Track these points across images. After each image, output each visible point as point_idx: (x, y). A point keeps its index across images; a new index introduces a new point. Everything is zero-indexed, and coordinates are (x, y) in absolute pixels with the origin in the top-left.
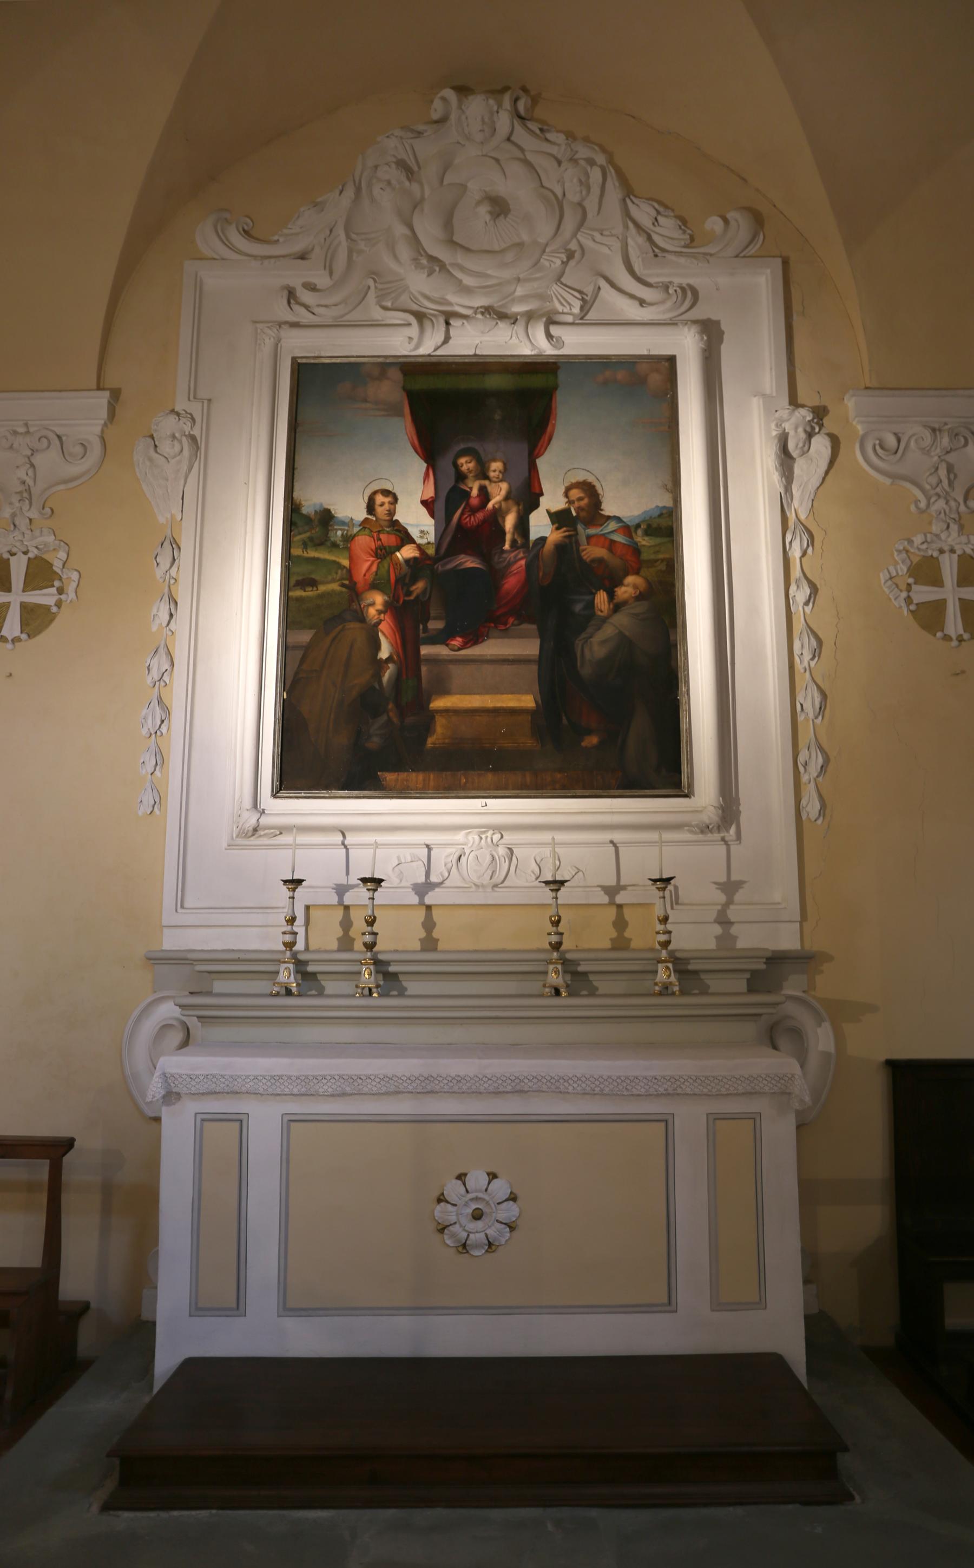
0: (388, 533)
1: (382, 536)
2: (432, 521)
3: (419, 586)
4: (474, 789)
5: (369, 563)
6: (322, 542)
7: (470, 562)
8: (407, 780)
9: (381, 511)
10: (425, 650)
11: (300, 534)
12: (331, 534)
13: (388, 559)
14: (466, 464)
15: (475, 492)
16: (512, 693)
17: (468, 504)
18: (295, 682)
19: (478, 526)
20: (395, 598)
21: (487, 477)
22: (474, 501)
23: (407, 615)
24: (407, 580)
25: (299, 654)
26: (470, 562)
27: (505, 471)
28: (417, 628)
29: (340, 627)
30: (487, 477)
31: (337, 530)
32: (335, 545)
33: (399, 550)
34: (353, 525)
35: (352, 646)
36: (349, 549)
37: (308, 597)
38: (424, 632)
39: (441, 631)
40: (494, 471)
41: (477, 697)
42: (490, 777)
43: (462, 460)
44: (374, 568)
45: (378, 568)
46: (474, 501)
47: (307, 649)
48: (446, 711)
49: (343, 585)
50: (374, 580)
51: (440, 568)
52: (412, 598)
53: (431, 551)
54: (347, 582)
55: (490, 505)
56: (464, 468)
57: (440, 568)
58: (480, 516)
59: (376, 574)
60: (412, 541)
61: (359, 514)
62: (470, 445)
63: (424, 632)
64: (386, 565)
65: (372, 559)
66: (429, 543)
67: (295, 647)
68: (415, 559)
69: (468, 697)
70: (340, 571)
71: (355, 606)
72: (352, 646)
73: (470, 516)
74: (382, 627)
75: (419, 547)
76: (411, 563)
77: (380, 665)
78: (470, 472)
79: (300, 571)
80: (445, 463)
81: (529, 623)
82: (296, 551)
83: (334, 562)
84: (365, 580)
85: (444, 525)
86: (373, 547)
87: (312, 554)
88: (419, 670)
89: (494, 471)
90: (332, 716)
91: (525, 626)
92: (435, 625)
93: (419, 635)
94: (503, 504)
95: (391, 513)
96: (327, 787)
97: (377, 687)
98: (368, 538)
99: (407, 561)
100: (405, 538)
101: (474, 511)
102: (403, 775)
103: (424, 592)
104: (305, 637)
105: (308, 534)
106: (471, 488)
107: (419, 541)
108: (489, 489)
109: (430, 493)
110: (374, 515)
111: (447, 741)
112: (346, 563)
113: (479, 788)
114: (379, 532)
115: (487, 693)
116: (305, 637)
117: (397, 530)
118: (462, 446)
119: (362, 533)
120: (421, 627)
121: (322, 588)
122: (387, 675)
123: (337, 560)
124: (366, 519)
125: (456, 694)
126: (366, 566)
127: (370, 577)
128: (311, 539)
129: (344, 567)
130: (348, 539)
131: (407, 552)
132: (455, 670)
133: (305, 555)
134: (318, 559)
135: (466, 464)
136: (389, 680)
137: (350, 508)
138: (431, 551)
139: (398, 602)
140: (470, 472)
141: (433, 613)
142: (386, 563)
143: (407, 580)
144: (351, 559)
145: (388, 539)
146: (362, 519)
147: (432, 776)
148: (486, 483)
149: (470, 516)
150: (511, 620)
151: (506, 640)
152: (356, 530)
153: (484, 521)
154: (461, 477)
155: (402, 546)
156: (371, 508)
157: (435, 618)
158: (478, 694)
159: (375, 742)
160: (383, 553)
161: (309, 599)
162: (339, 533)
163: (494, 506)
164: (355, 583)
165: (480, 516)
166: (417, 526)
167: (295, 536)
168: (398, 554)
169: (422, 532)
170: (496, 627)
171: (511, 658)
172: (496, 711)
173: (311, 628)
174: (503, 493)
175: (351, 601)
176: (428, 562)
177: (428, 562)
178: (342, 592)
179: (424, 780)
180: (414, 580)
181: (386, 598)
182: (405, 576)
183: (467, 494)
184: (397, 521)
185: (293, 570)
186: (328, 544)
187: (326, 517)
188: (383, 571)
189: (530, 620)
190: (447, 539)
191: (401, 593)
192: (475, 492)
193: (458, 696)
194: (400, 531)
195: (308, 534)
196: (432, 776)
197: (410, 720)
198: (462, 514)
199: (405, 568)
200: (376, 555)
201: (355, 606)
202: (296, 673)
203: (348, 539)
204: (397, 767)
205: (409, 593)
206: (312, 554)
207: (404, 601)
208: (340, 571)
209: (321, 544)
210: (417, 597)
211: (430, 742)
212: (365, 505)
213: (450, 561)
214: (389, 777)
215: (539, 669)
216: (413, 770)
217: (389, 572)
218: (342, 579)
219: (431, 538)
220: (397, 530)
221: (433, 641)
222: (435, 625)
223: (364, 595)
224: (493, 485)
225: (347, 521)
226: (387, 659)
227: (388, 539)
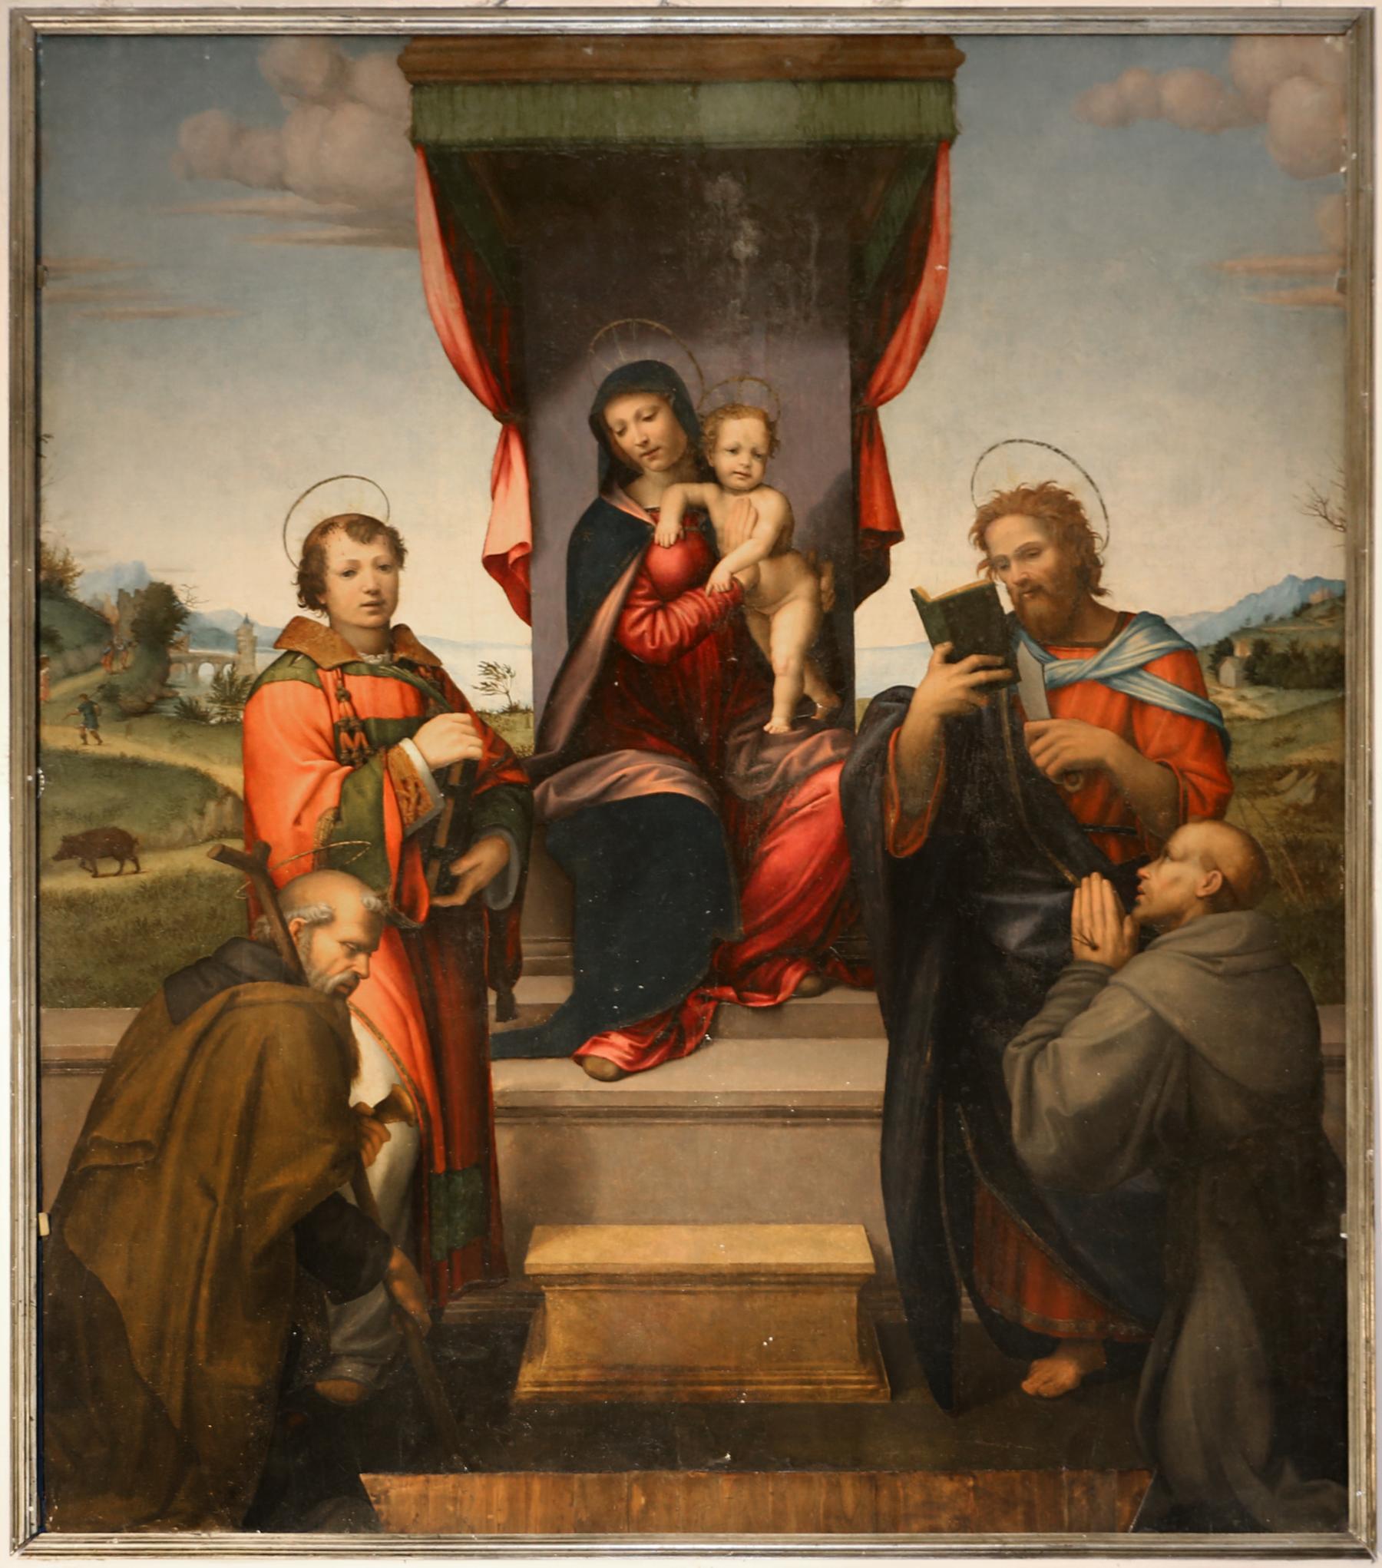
0: (373, 671)
1: (353, 683)
2: (523, 632)
3: (483, 860)
4: (672, 1528)
5: (311, 779)
6: (147, 703)
7: (651, 776)
8: (455, 1500)
9: (348, 596)
10: (509, 1078)
11: (71, 674)
12: (178, 675)
13: (375, 764)
14: (638, 423)
15: (667, 528)
16: (797, 1220)
17: (643, 570)
18: (77, 1180)
19: (680, 650)
20: (403, 902)
21: (708, 474)
22: (667, 560)
23: (445, 954)
24: (441, 841)
25: (87, 1089)
26: (651, 776)
27: (772, 447)
28: (480, 1001)
29: (222, 997)
30: (708, 474)
31: (197, 660)
32: (191, 715)
33: (411, 734)
34: (254, 642)
35: (261, 1064)
36: (236, 728)
37: (105, 894)
38: (502, 1017)
39: (561, 1013)
40: (734, 451)
41: (683, 1232)
42: (725, 1489)
43: (623, 411)
44: (329, 796)
45: (343, 796)
46: (667, 560)
47: (113, 1071)
48: (581, 1279)
49: (224, 855)
50: (331, 837)
51: (551, 795)
52: (459, 899)
53: (521, 738)
54: (237, 845)
55: (719, 578)
56: (630, 441)
57: (551, 795)
58: (687, 611)
59: (337, 817)
60: (459, 704)
61: (277, 605)
62: (650, 353)
63: (502, 1017)
64: (369, 787)
65: (322, 764)
66: (513, 709)
67: (71, 1067)
68: (468, 765)
69: (650, 1233)
70: (211, 807)
71: (267, 926)
72: (261, 1064)
73: (652, 612)
74: (357, 998)
75: (481, 723)
76: (455, 780)
77: (355, 1129)
78: (652, 453)
79: (77, 804)
80: (564, 419)
81: (854, 986)
82: (61, 737)
83: (192, 773)
84: (301, 836)
85: (565, 645)
86: (325, 725)
87: (116, 744)
88: (488, 1143)
89: (734, 451)
90: (205, 1292)
91: (838, 997)
92: (540, 993)
93: (484, 1027)
94: (767, 574)
95: (383, 602)
96: (194, 1521)
97: (352, 1200)
98: (304, 690)
99: (440, 774)
100: (435, 692)
101: (665, 594)
102: (442, 1484)
103: (500, 878)
104: (102, 1031)
105: (98, 676)
106: (654, 513)
107: (479, 701)
108: (718, 516)
109: (514, 531)
110: (325, 608)
111: (584, 1374)
112: (230, 776)
113: (689, 1526)
114: (343, 667)
115: (715, 1221)
116: (102, 1031)
117: (403, 663)
118: (624, 357)
119: (285, 670)
120: (492, 998)
121: (155, 866)
122: (386, 1157)
123: (202, 766)
124: (298, 621)
125: (611, 1222)
126: (299, 792)
127: (316, 827)
128: (110, 693)
129: (229, 792)
130: (238, 692)
131: (442, 742)
132: (609, 1145)
133: (92, 748)
134: (137, 765)
135: (638, 423)
136: (389, 1179)
137: (240, 587)
138: (521, 738)
139: (412, 912)
140: (652, 453)
141: (531, 950)
142: (367, 779)
143: (441, 841)
144: (249, 765)
145: (377, 696)
146: (282, 623)
147: (537, 1487)
148: (706, 492)
149: (652, 612)
150: (792, 977)
151: (775, 1043)
152: (264, 659)
153: (700, 633)
154: (619, 472)
155: (423, 719)
156: (312, 585)
157: (539, 970)
158: (685, 1222)
159: (346, 1380)
160: (359, 744)
161: (115, 903)
162: (207, 671)
163: (733, 580)
164: (267, 848)
165: (687, 611)
166: (473, 647)
167: (55, 680)
168: (407, 745)
169: (490, 669)
170: (741, 1000)
171: (792, 1103)
172: (744, 1279)
173: (121, 1002)
174: (766, 531)
175: (253, 910)
176: (511, 776)
177: (511, 776)
178: (221, 879)
179: (512, 1499)
180: (465, 837)
181: (372, 900)
182: (433, 825)
183: (641, 536)
184: (402, 629)
185: (57, 799)
186: (170, 709)
187: (159, 617)
188: (360, 806)
189: (856, 976)
190: (578, 695)
191: (422, 883)
192: (667, 528)
193: (619, 1229)
194: (409, 665)
195: (98, 676)
196: (537, 1487)
197: (459, 1308)
198: (626, 605)
199: (435, 800)
200: (336, 752)
201: (267, 926)
202: (79, 1153)
203: (238, 692)
204: (426, 1455)
205: (449, 884)
206: (116, 744)
207: (433, 909)
208: (211, 807)
209: (147, 710)
210: (477, 896)
211: (530, 1377)
212: (291, 573)
213: (585, 774)
214: (394, 1489)
215: (885, 1140)
216: (474, 1468)
217: (378, 808)
218: (224, 834)
219: (522, 690)
220: (403, 663)
221: (534, 1044)
222: (540, 993)
223: (297, 891)
224: (731, 499)
225: (231, 628)
226: (382, 1107)
227: (377, 696)
